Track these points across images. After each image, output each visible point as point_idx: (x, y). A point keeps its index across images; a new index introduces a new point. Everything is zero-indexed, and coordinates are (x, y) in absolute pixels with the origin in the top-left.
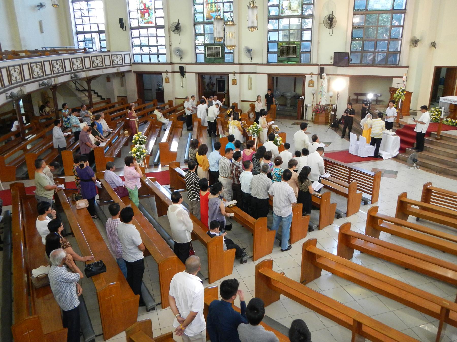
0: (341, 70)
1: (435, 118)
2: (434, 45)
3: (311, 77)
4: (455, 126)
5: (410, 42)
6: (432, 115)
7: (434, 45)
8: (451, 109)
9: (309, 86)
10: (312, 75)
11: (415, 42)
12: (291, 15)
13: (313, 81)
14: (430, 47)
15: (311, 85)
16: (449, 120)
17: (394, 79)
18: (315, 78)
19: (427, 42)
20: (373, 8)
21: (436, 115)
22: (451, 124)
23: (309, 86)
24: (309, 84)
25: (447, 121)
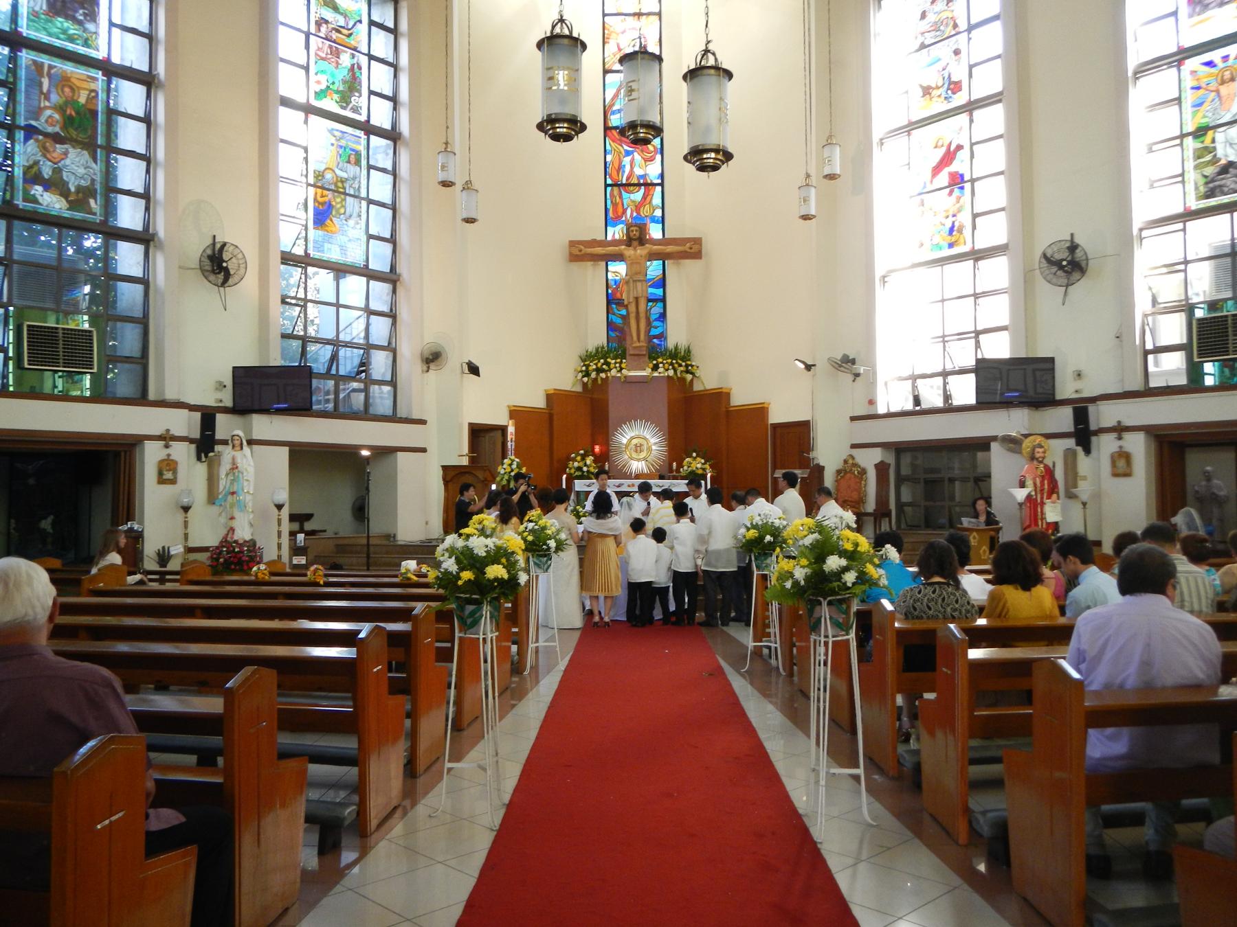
0: (263, 426)
3: (167, 446)
9: (161, 481)
10: (167, 438)
11: (432, 359)
12: (67, 214)
13: (176, 463)
15: (168, 475)
17: (399, 454)
18: (183, 453)
23: (161, 481)
24: (160, 473)
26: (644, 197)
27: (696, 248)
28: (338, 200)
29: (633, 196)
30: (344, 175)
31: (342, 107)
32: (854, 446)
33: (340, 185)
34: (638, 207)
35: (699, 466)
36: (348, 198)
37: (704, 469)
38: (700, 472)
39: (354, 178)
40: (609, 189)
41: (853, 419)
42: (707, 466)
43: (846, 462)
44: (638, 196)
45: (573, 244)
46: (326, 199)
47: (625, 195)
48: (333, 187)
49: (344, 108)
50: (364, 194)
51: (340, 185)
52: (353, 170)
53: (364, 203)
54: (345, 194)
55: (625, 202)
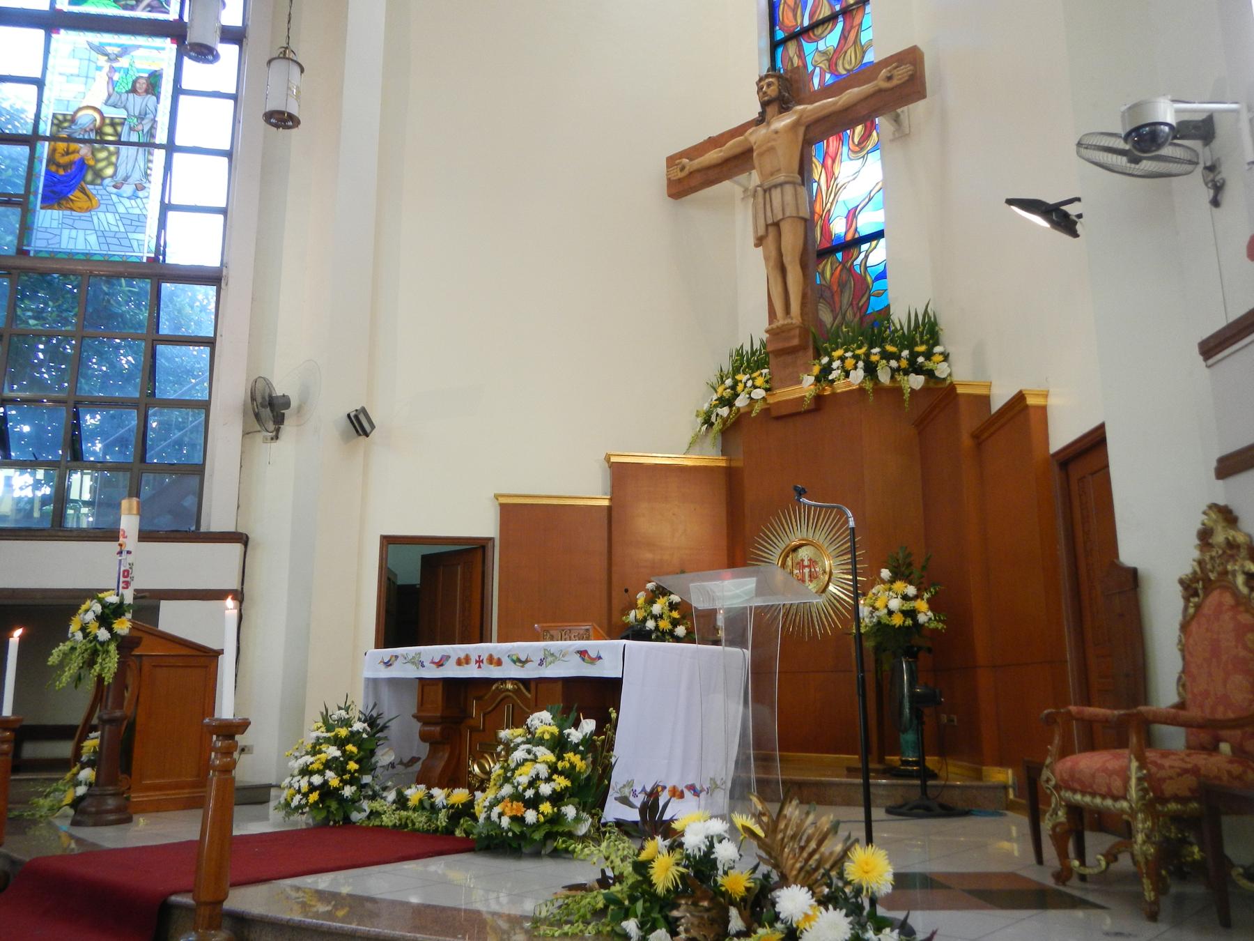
1: (324, 789)
2: (359, 424)
4: (449, 831)
5: (245, 414)
6: (306, 771)
7: (359, 424)
8: (425, 721)
11: (269, 411)
14: (346, 438)
16: (415, 793)
17: (163, 603)
19: (328, 412)
20: (54, 247)
21: (328, 765)
22: (420, 820)
25: (402, 802)
26: (844, 37)
27: (902, 73)
28: (103, 155)
29: (822, 45)
30: (120, 114)
31: (126, 7)
32: (1229, 467)
33: (108, 130)
34: (832, 60)
35: (895, 604)
36: (123, 149)
37: (911, 614)
38: (897, 620)
39: (141, 117)
40: (780, 51)
41: (1211, 348)
42: (922, 605)
43: (1205, 536)
44: (831, 39)
45: (672, 161)
46: (75, 157)
47: (808, 47)
48: (93, 136)
49: (132, 8)
50: (161, 137)
51: (108, 130)
52: (137, 103)
53: (159, 156)
54: (119, 142)
55: (809, 60)
